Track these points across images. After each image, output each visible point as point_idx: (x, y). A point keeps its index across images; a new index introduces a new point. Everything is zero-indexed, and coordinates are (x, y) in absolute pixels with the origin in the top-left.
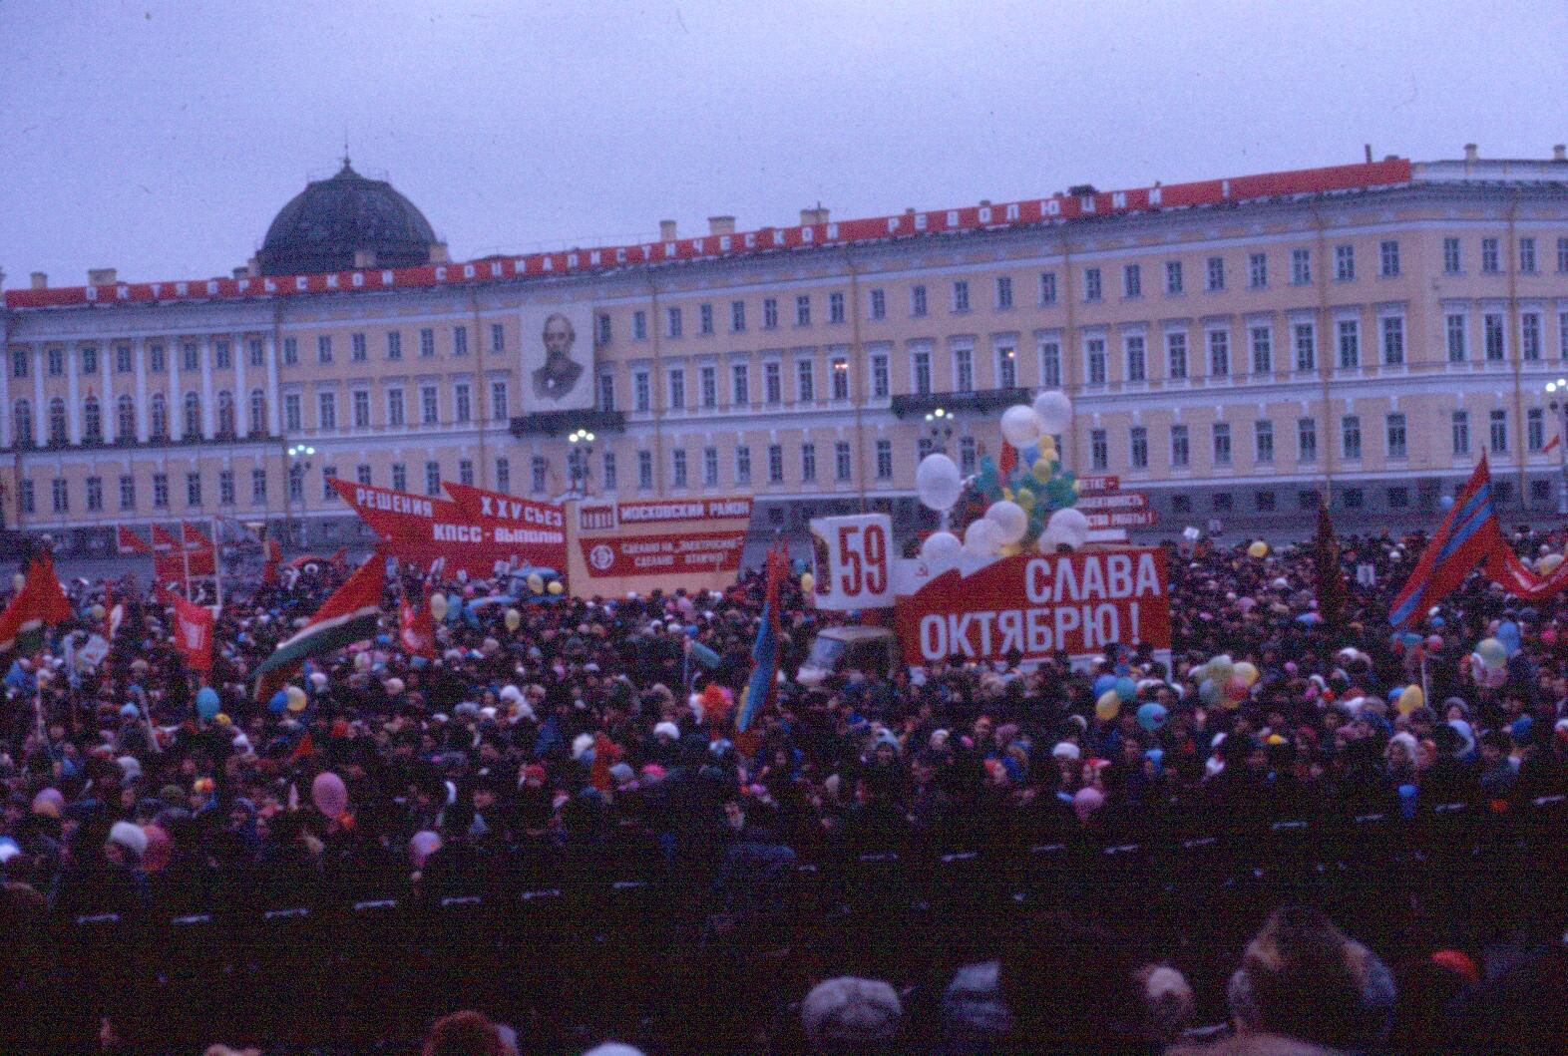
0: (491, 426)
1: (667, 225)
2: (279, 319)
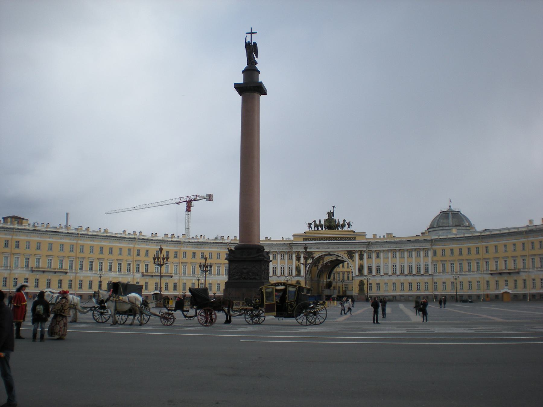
0: (485, 272)
1: (531, 221)
2: (432, 245)
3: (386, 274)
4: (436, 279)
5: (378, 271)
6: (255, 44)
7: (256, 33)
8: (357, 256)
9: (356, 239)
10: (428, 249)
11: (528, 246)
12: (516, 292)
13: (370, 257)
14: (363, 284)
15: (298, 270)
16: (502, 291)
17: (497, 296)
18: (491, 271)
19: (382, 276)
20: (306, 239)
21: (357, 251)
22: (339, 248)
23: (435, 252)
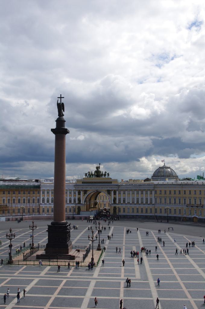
3: (129, 203)
4: (156, 207)
5: (124, 201)
6: (63, 104)
7: (64, 98)
8: (112, 193)
9: (112, 183)
10: (152, 190)
12: (201, 217)
13: (120, 193)
15: (79, 200)
16: (193, 216)
18: (187, 204)
19: (126, 204)
21: (112, 190)
22: (102, 188)
23: (156, 192)
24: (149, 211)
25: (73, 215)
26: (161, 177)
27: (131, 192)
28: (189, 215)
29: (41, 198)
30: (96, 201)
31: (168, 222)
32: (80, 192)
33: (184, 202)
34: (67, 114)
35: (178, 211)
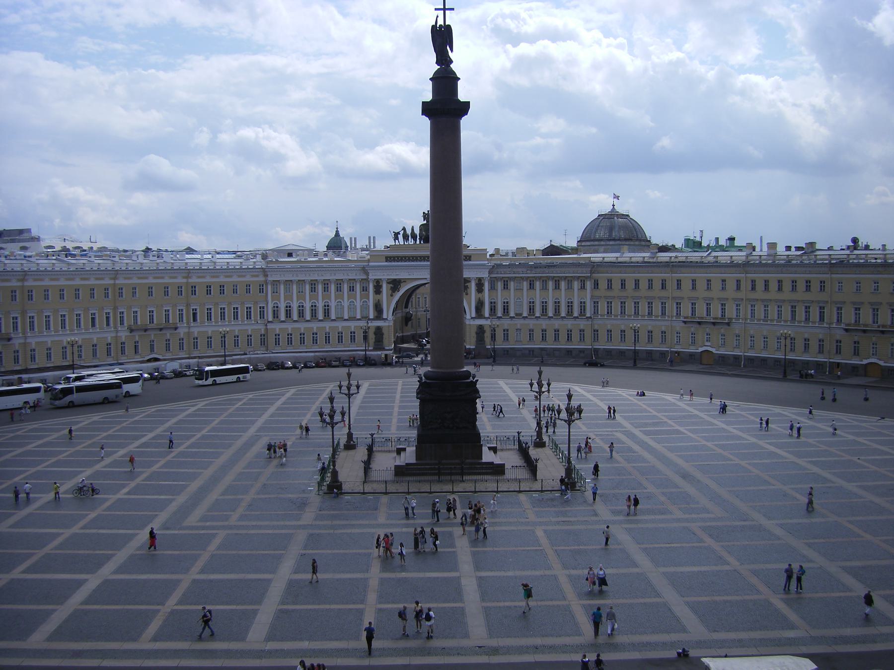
3: (521, 314)
4: (598, 323)
5: (506, 310)
6: (449, 26)
7: (453, 9)
10: (587, 277)
11: (746, 286)
12: (722, 352)
13: (492, 288)
14: (484, 332)
16: (701, 350)
17: (692, 355)
18: (685, 318)
20: (390, 257)
23: (596, 285)
24: (576, 336)
25: (365, 350)
26: (608, 243)
27: (525, 283)
28: (692, 347)
29: (270, 306)
30: (407, 310)
31: (635, 364)
32: (381, 287)
33: (749, 312)
34: (461, 58)
35: (657, 336)
